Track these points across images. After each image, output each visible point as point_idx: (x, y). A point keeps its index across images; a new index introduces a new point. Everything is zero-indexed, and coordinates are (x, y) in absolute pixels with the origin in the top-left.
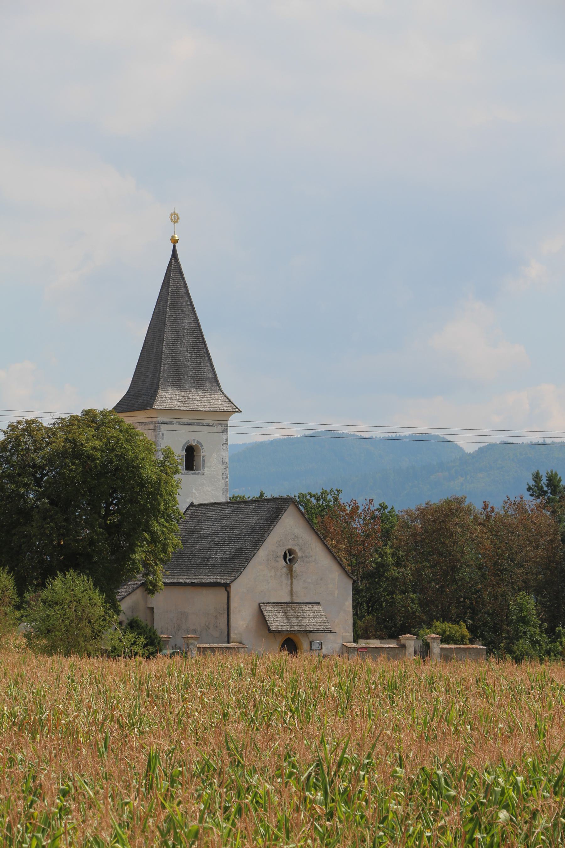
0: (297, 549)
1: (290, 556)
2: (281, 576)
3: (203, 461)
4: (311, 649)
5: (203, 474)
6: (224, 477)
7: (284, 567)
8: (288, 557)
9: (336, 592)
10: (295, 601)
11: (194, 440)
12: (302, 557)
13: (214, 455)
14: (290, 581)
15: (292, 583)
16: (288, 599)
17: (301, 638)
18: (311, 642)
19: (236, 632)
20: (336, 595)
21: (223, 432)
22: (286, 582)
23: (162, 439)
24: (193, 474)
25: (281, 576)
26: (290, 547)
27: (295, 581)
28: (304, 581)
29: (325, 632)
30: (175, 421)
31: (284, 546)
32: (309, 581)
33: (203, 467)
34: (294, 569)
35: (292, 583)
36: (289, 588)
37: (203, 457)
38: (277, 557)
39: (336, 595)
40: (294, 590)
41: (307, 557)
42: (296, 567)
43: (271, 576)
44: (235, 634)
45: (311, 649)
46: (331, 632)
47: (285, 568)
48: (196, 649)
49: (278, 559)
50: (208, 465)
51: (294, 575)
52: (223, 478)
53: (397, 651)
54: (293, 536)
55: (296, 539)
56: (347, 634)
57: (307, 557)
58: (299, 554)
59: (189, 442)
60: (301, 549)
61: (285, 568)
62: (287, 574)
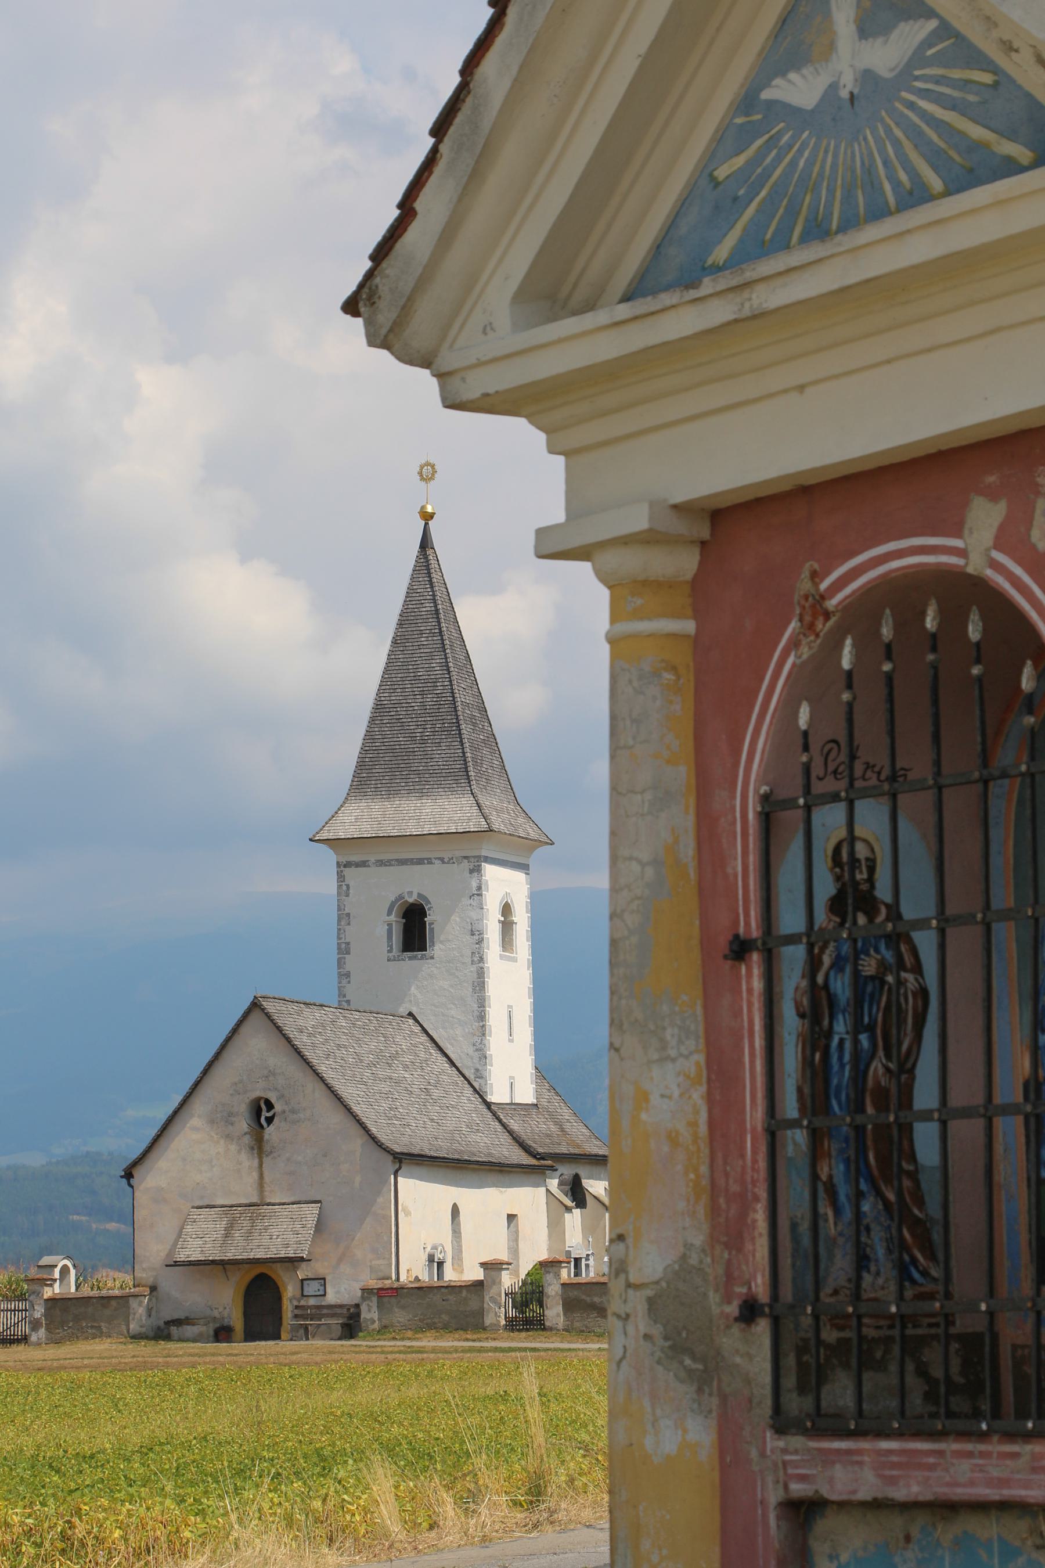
1: (268, 1111)
3: (432, 930)
4: (303, 1295)
5: (432, 958)
8: (265, 1114)
9: (358, 1179)
10: (268, 1201)
11: (410, 893)
12: (284, 1112)
13: (455, 918)
14: (256, 1162)
16: (255, 1199)
17: (282, 1273)
19: (144, 1266)
21: (471, 871)
22: (248, 1162)
23: (348, 896)
24: (410, 958)
26: (258, 1094)
28: (288, 1159)
30: (372, 859)
32: (300, 1158)
33: (433, 944)
34: (266, 1137)
36: (255, 1175)
37: (431, 924)
38: (231, 1114)
41: (293, 1111)
42: (270, 1132)
43: (218, 1153)
44: (144, 1270)
45: (303, 1295)
47: (248, 1136)
48: (42, 1302)
49: (234, 1119)
50: (442, 938)
51: (267, 1148)
53: (464, 1293)
54: (266, 1072)
56: (381, 1262)
57: (293, 1111)
58: (278, 1107)
59: (401, 897)
60: (281, 1097)
61: (248, 1136)
62: (252, 1148)
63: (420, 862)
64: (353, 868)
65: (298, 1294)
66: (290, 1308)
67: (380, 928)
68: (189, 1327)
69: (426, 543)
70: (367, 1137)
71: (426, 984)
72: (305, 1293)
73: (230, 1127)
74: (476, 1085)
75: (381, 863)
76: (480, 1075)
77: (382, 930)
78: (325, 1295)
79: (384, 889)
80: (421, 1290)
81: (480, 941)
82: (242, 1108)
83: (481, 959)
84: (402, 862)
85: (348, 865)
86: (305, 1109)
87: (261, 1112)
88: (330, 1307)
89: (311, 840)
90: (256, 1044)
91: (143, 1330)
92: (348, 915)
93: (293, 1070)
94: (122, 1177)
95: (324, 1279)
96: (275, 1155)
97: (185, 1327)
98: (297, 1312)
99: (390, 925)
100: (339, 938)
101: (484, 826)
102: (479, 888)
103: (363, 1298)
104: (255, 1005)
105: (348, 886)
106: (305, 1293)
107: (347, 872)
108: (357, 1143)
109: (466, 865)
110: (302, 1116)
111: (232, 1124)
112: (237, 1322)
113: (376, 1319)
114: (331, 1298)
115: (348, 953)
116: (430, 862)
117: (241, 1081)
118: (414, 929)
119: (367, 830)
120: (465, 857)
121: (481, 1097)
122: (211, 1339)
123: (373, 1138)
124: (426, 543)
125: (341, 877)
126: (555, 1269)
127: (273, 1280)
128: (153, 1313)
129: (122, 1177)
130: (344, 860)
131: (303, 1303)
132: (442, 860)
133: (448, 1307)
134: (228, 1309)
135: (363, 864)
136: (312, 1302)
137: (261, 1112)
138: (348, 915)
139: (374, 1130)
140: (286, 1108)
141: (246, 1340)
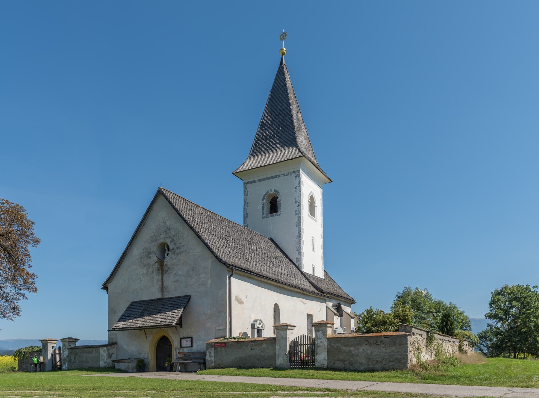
0: (168, 241)
2: (153, 272)
3: (280, 204)
6: (297, 213)
7: (156, 262)
8: (167, 252)
9: (209, 282)
11: (271, 190)
14: (160, 276)
15: (162, 279)
17: (171, 335)
18: (181, 339)
20: (209, 285)
21: (296, 177)
22: (157, 277)
25: (153, 272)
26: (161, 241)
27: (165, 276)
28: (175, 274)
31: (156, 241)
32: (181, 273)
34: (165, 263)
35: (162, 279)
36: (160, 283)
39: (209, 285)
40: (165, 285)
43: (144, 274)
45: (181, 347)
47: (157, 264)
49: (151, 255)
52: (296, 214)
55: (168, 232)
57: (178, 248)
58: (171, 247)
59: (268, 192)
61: (157, 264)
62: (159, 270)
63: (275, 177)
64: (250, 184)
65: (179, 346)
67: (260, 205)
68: (123, 364)
69: (281, 73)
70: (214, 258)
71: (276, 225)
73: (149, 260)
74: (297, 264)
75: (260, 180)
76: (299, 260)
77: (260, 207)
78: (192, 346)
79: (262, 190)
80: (241, 343)
81: (299, 205)
82: (154, 248)
83: (300, 213)
84: (268, 178)
85: (248, 183)
86: (183, 246)
87: (164, 249)
89: (233, 174)
90: (161, 214)
91: (106, 364)
92: (248, 203)
93: (179, 226)
94: (102, 288)
95: (192, 338)
96: (169, 272)
98: (179, 356)
99: (263, 204)
100: (244, 212)
101: (301, 154)
102: (299, 183)
103: (207, 349)
104: (160, 193)
105: (248, 192)
107: (247, 186)
108: (209, 262)
109: (294, 175)
110: (182, 250)
111: (150, 258)
112: (152, 362)
113: (213, 360)
115: (247, 217)
116: (279, 176)
117: (154, 235)
118: (273, 206)
119: (254, 165)
120: (294, 172)
121: (299, 269)
122: (135, 370)
123: (217, 257)
124: (281, 73)
125: (245, 188)
126: (323, 328)
129: (102, 288)
130: (246, 181)
131: (181, 351)
132: (284, 175)
133: (257, 354)
135: (254, 182)
136: (186, 350)
137: (164, 249)
138: (248, 203)
139: (218, 254)
140: (174, 247)
141: (157, 371)
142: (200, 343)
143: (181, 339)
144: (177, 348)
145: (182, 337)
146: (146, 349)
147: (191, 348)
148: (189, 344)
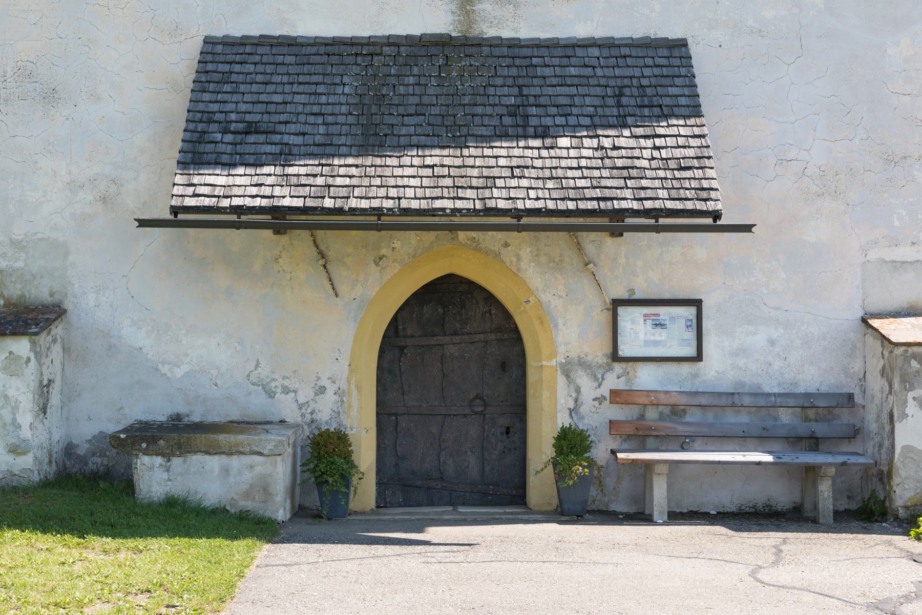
4: (615, 357)
17: (533, 275)
29: (656, 220)
45: (615, 357)
46: (713, 222)
65: (597, 351)
66: (564, 401)
68: (214, 463)
72: (625, 350)
78: (699, 357)
88: (729, 400)
95: (697, 303)
97: (197, 459)
106: (625, 350)
114: (720, 367)
127: (490, 298)
128: (55, 399)
134: (330, 397)
136: (647, 378)
142: (758, 339)
143: (617, 303)
144: (583, 364)
145: (621, 293)
146: (310, 353)
147: (685, 369)
148: (678, 342)
